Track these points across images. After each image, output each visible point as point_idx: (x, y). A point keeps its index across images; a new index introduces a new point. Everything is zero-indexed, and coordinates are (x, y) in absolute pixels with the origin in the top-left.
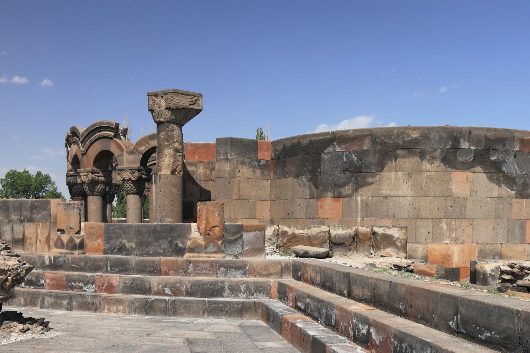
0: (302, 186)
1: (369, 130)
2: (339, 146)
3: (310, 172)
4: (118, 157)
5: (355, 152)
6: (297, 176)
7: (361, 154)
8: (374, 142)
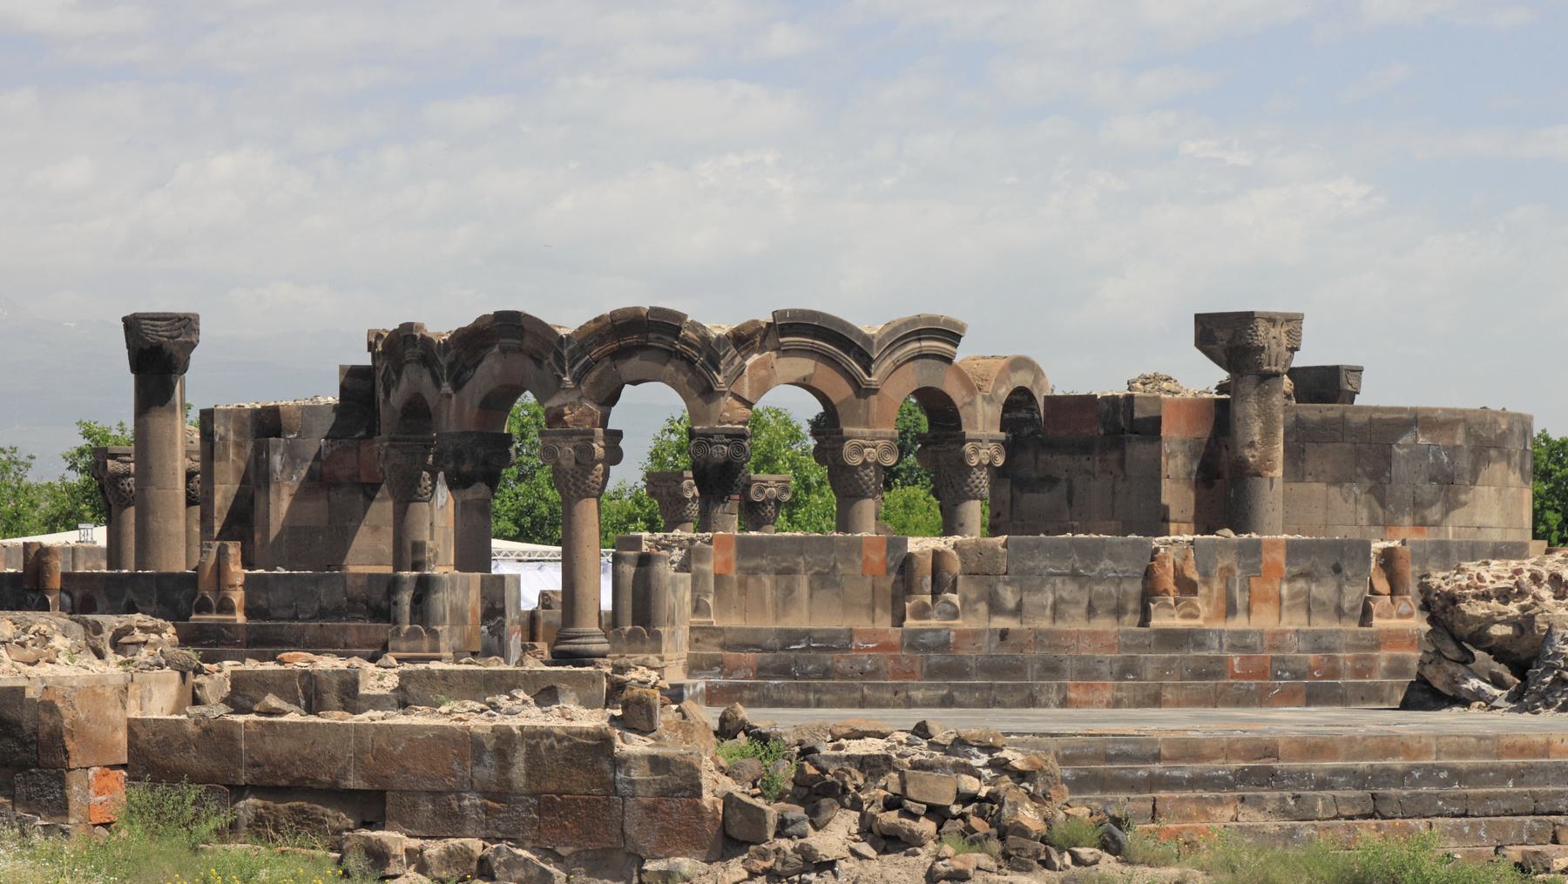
0: (1352, 500)
1: (1463, 412)
2: (1423, 435)
3: (1372, 476)
4: (961, 407)
5: (1446, 448)
6: (1337, 482)
7: (1453, 451)
8: (1468, 433)
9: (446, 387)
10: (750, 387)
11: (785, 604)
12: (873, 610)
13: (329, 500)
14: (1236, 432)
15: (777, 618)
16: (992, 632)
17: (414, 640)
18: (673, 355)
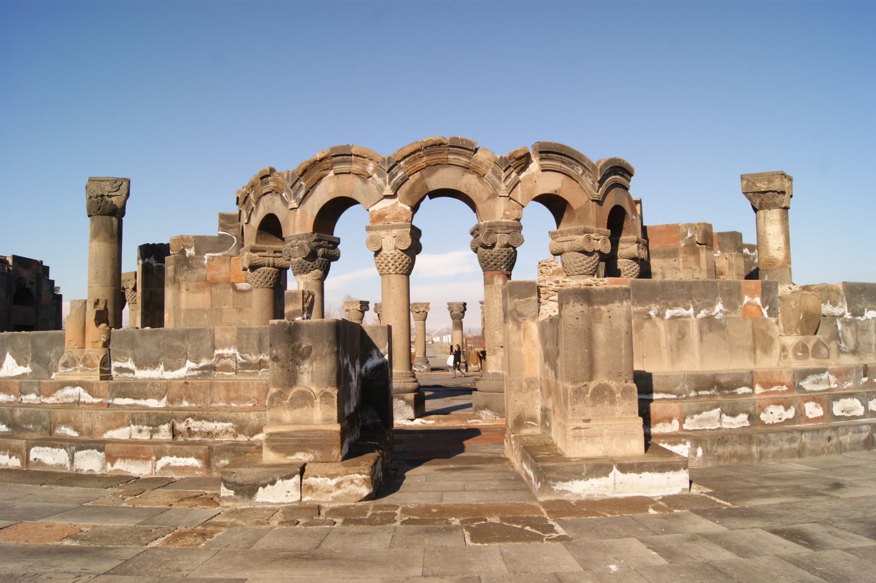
9: (293, 204)
10: (522, 194)
11: (678, 348)
12: (755, 353)
13: (211, 292)
15: (673, 362)
16: (857, 367)
17: (301, 406)
18: (466, 168)
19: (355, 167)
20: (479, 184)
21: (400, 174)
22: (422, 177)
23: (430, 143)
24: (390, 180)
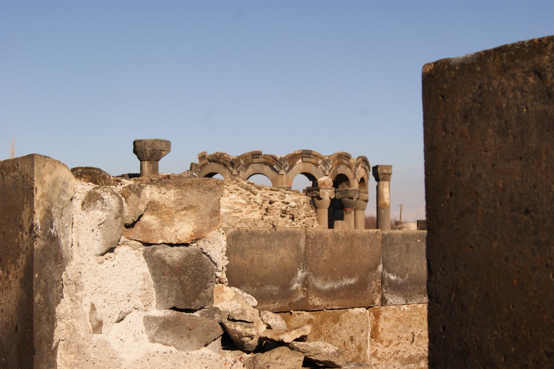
14: (384, 196)
19: (313, 160)
20: (351, 173)
21: (331, 166)
22: (336, 168)
23: (340, 154)
24: (328, 168)
